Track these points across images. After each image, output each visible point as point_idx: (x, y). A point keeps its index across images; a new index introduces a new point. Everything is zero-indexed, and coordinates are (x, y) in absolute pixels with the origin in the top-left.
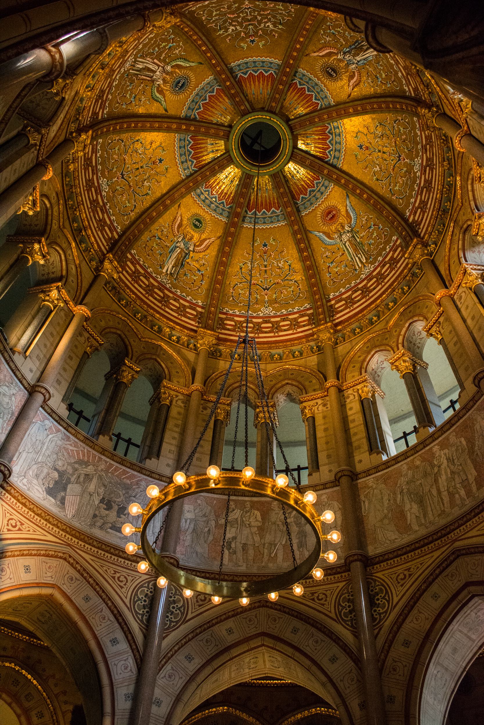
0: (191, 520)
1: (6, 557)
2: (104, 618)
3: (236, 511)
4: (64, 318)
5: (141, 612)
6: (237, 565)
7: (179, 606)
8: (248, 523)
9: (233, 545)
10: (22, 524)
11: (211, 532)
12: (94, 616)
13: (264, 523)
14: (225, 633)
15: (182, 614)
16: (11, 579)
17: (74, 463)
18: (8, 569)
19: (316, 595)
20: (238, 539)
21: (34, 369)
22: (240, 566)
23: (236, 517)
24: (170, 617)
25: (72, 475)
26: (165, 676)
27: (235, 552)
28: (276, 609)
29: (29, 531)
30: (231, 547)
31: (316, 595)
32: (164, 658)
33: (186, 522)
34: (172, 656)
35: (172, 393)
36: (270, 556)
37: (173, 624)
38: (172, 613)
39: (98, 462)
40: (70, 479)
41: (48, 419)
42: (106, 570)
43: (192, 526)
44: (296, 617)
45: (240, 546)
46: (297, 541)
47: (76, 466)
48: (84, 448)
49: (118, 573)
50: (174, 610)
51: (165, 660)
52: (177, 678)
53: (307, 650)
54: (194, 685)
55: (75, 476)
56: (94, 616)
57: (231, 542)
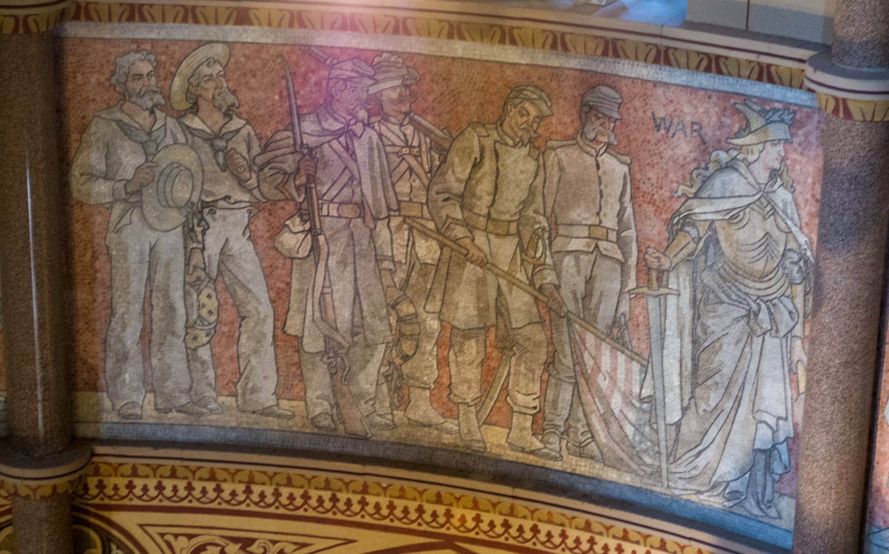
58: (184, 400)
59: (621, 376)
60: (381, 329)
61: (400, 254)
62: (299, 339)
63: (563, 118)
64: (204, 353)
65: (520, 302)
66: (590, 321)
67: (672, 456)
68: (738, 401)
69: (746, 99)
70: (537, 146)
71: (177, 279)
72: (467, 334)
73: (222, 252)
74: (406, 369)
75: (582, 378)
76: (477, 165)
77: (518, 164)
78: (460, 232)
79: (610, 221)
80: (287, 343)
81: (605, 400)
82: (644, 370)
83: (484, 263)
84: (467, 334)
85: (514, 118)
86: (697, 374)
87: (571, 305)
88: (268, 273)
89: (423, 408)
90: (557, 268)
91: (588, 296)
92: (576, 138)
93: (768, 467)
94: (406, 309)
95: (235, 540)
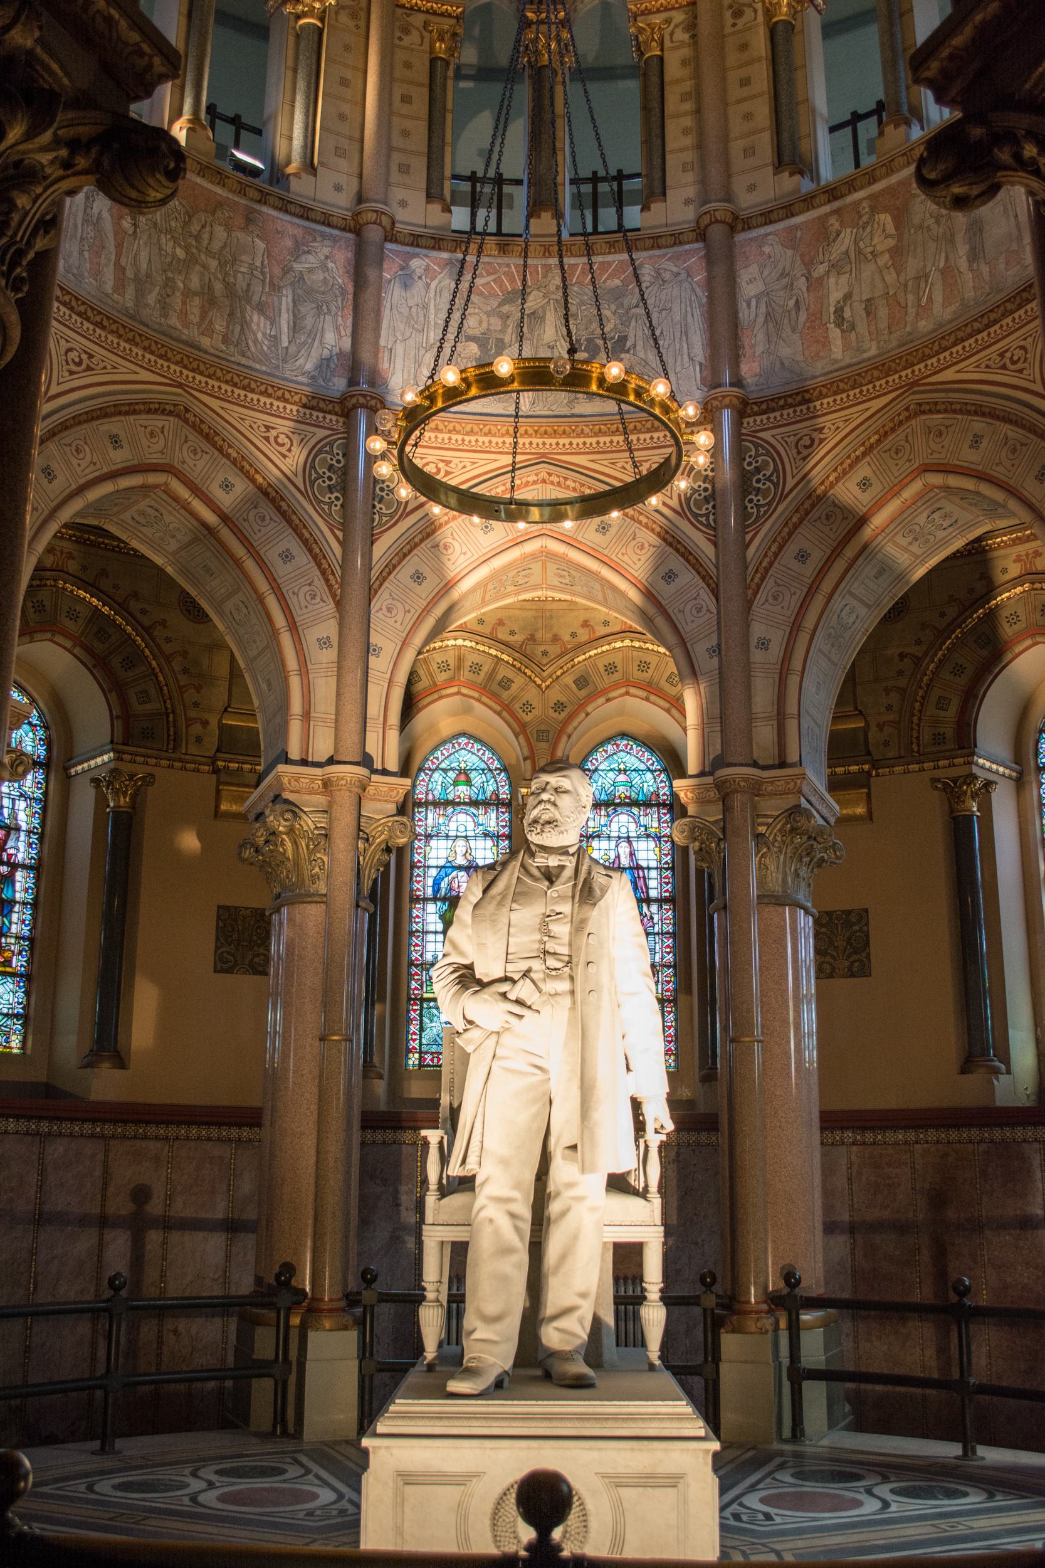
0: (758, 297)
1: (441, 525)
2: (643, 545)
3: (842, 235)
4: (351, 23)
5: (704, 511)
6: (859, 350)
7: (768, 474)
8: (871, 249)
9: (847, 314)
10: (447, 463)
11: (803, 307)
12: (623, 550)
13: (900, 238)
14: (856, 491)
15: (776, 485)
16: (465, 553)
17: (499, 306)
18: (454, 542)
19: (1008, 355)
20: (855, 297)
21: (343, 180)
22: (865, 351)
23: (843, 248)
24: (755, 499)
25: (503, 331)
26: (767, 601)
27: (853, 327)
28: (939, 412)
29: (464, 467)
30: (843, 319)
31: (1008, 355)
32: (756, 572)
33: (749, 306)
34: (771, 564)
35: (657, 19)
36: (919, 306)
37: (762, 510)
38: (758, 491)
39: (545, 276)
40: (502, 340)
41: (417, 255)
42: (623, 467)
43: (763, 309)
44: (976, 413)
45: (859, 308)
46: (967, 247)
47: (506, 309)
48: (508, 265)
49: (646, 461)
50: (760, 485)
51: (759, 575)
52: (788, 597)
53: (998, 472)
54: (819, 600)
55: (510, 330)
56: (623, 550)
57: (842, 309)
58: (75, 271)
59: (262, 325)
60: (159, 279)
61: (169, 250)
62: (124, 269)
63: (239, 221)
64: (86, 254)
65: (218, 287)
66: (249, 301)
67: (285, 361)
68: (314, 340)
69: (314, 230)
70: (229, 228)
71: (80, 214)
72: (195, 294)
73: (99, 213)
74: (168, 300)
75: (245, 324)
76: (203, 227)
77: (220, 232)
78: (194, 250)
79: (258, 263)
80: (120, 269)
81: (255, 334)
82: (272, 324)
83: (204, 267)
84: (195, 294)
85: (219, 214)
86: (295, 328)
87: (240, 293)
88: (116, 234)
89: (174, 321)
90: (235, 277)
91: (248, 291)
92: (244, 229)
93: (328, 366)
94: (170, 275)
95: (86, 352)
